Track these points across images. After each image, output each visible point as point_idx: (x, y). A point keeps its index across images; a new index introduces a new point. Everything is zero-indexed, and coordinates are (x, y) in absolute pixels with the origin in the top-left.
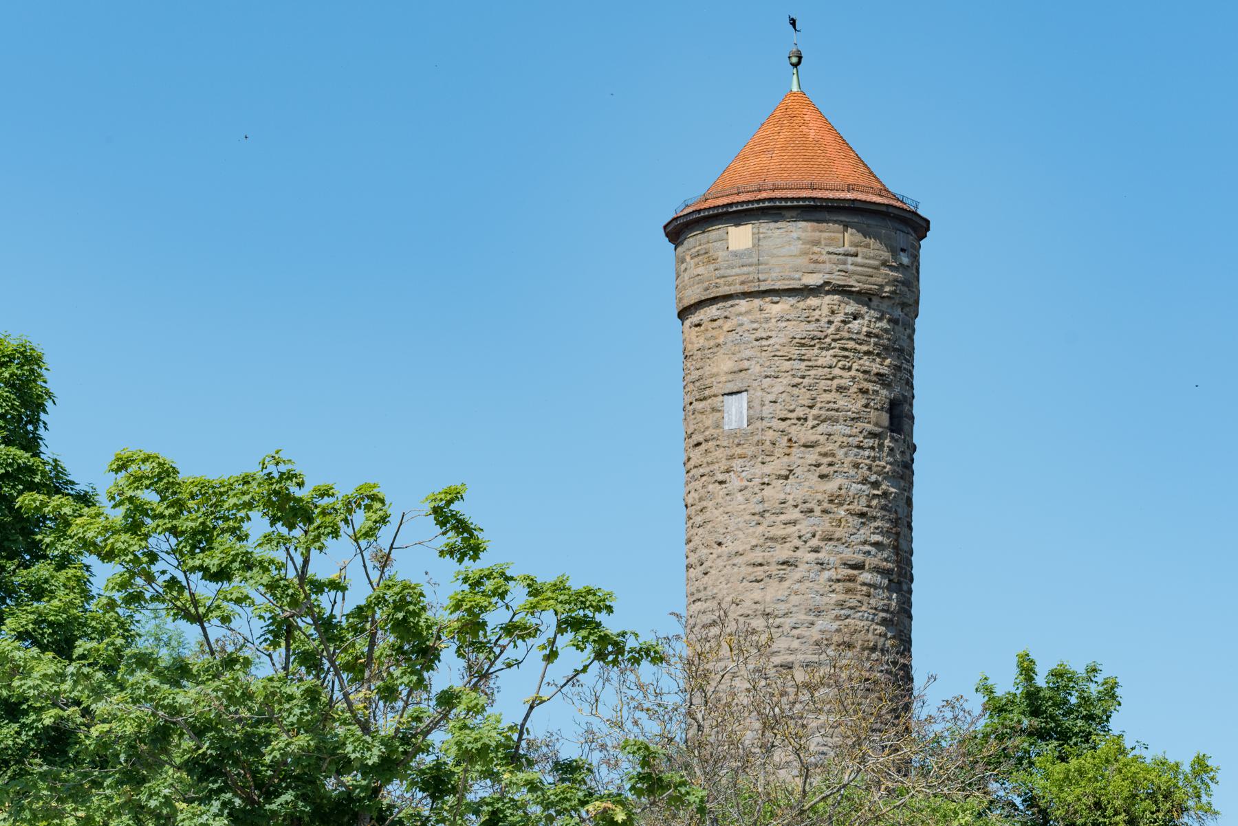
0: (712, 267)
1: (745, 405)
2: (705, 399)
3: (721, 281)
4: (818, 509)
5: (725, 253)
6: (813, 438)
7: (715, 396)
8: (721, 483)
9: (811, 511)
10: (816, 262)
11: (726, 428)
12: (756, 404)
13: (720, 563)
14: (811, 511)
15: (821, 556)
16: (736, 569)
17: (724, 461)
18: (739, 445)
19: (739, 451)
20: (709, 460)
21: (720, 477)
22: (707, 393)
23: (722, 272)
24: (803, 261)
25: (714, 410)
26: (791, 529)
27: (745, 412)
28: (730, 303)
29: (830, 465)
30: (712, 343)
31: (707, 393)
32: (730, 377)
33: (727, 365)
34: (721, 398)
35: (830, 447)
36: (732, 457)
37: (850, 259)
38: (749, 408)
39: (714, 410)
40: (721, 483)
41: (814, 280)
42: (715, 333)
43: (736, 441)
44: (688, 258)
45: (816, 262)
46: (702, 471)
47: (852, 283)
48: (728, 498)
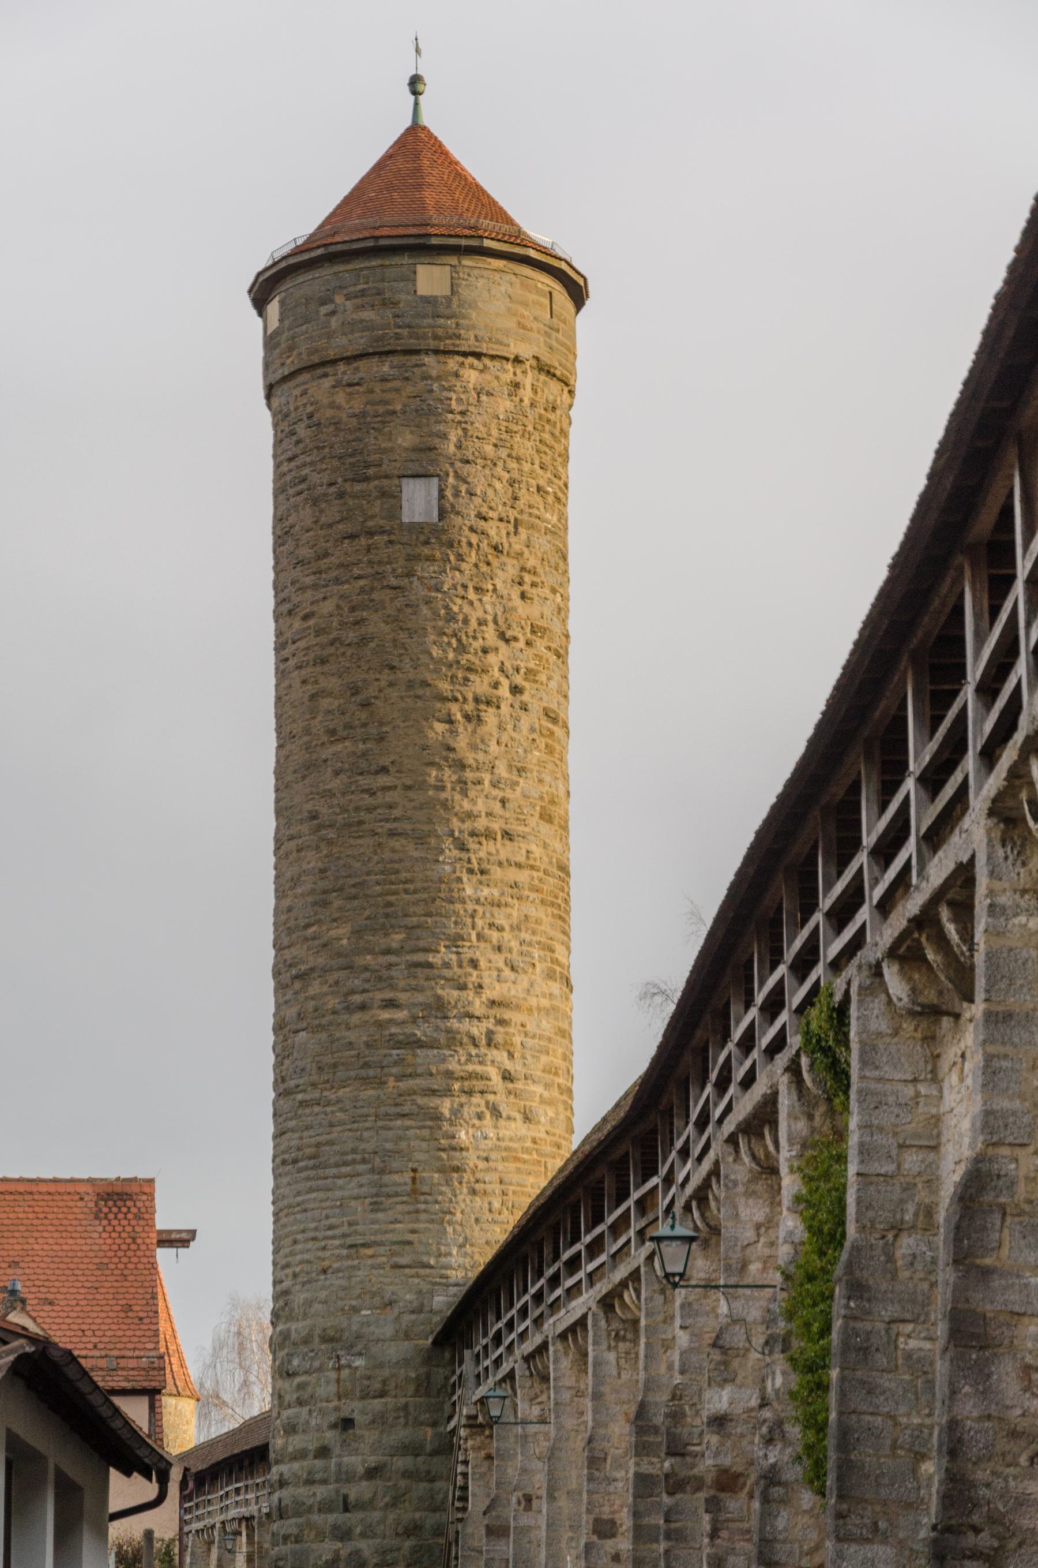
0: (389, 313)
1: (435, 493)
2: (367, 479)
3: (405, 332)
4: (521, 644)
5: (409, 298)
6: (517, 547)
7: (387, 477)
8: (395, 588)
9: (516, 639)
10: (524, 328)
11: (406, 519)
12: (449, 493)
13: (394, 694)
14: (516, 639)
15: (526, 697)
16: (420, 704)
17: (402, 562)
18: (427, 543)
19: (426, 551)
20: (376, 559)
21: (394, 582)
22: (371, 472)
23: (407, 320)
24: (511, 324)
25: (384, 494)
26: (492, 659)
27: (435, 503)
28: (414, 359)
29: (534, 585)
30: (381, 409)
31: (371, 472)
32: (414, 456)
33: (406, 439)
34: (396, 481)
35: (531, 563)
36: (417, 558)
37: (554, 334)
38: (442, 496)
39: (384, 494)
40: (395, 588)
41: (525, 351)
42: (388, 396)
43: (422, 538)
44: (339, 299)
45: (524, 328)
46: (356, 571)
47: (557, 365)
48: (409, 610)
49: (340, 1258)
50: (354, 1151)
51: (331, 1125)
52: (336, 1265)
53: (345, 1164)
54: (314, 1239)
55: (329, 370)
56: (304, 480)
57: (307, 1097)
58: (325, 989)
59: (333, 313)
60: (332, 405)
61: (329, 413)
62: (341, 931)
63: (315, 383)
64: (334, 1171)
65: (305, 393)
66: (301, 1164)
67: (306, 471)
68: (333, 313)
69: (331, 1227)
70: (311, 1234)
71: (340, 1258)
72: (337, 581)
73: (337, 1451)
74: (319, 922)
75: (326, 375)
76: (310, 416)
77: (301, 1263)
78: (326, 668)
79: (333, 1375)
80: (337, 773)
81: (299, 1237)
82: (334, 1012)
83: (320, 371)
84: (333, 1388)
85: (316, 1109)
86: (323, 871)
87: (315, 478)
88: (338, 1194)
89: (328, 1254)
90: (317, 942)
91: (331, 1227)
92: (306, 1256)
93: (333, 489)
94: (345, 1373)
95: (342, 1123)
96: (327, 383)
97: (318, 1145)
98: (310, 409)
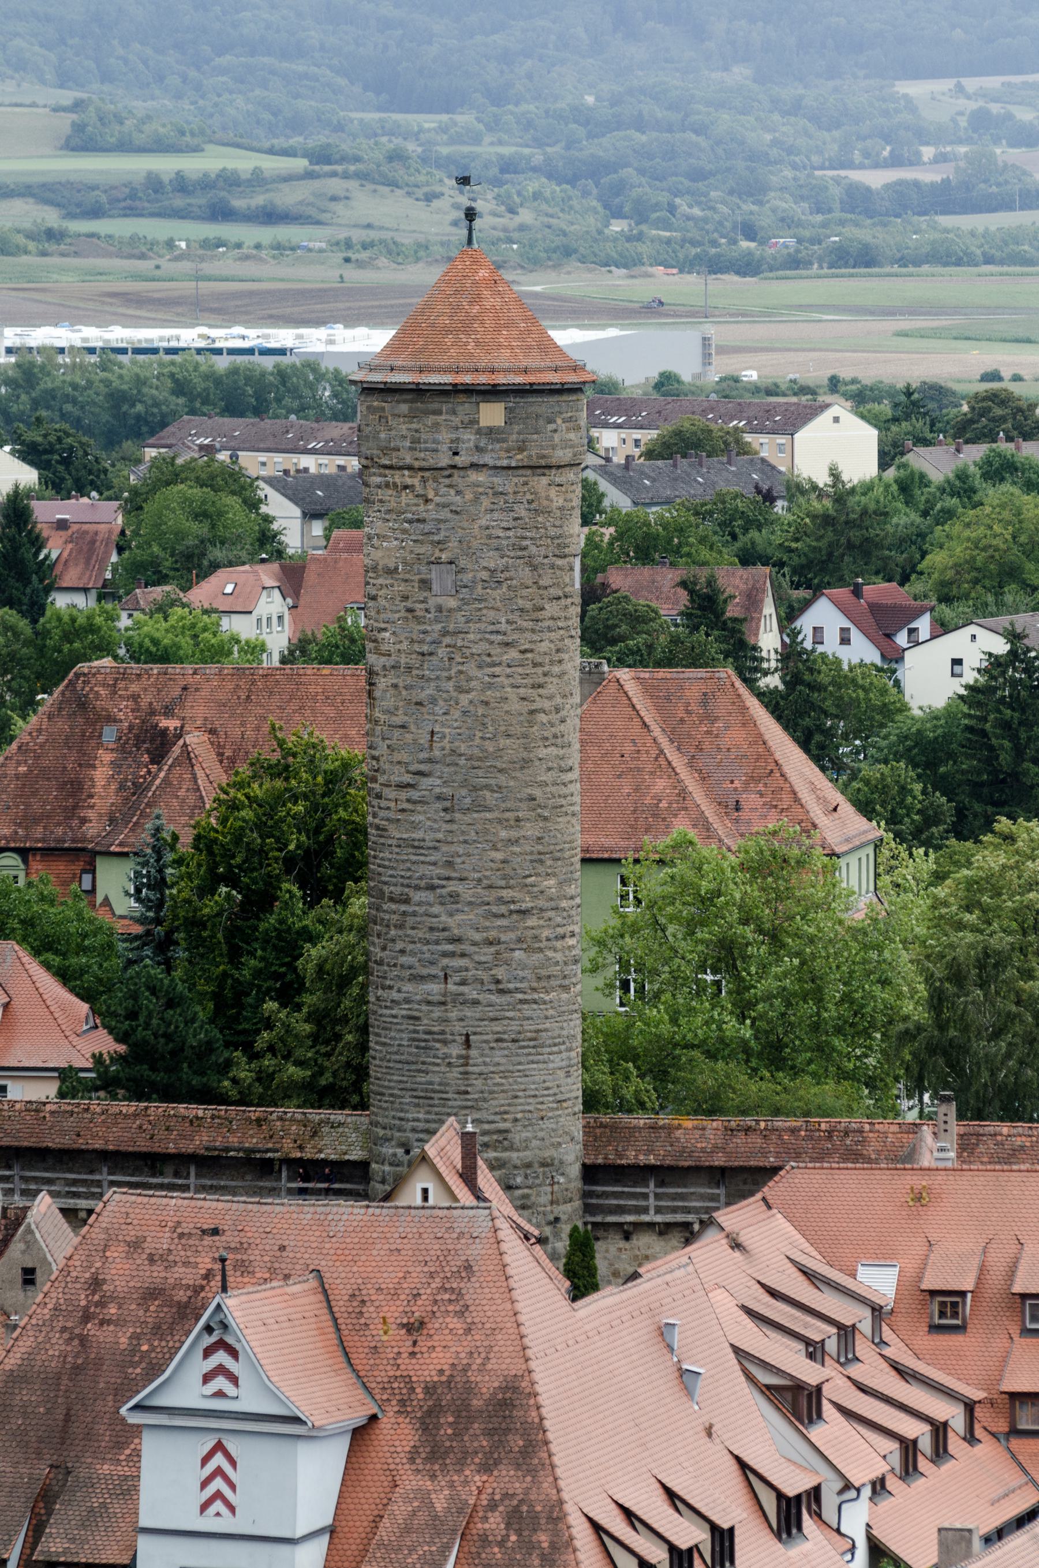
44: (559, 421)
49: (552, 1109)
50: (559, 1036)
51: (547, 1018)
52: (550, 1114)
53: (555, 1045)
54: (535, 1096)
55: (546, 471)
56: (525, 548)
57: (526, 997)
58: (541, 922)
59: (555, 431)
60: (548, 498)
61: (545, 503)
62: (552, 882)
63: (536, 478)
64: (548, 1050)
65: (526, 484)
66: (522, 1043)
67: (528, 542)
68: (555, 431)
69: (547, 1089)
70: (533, 1093)
71: (552, 1109)
72: (550, 629)
73: (551, 1239)
74: (537, 875)
75: (544, 475)
76: (530, 502)
77: (523, 1111)
78: (540, 691)
79: (549, 1189)
80: (549, 769)
81: (520, 1094)
82: (548, 940)
83: (539, 471)
84: (549, 1197)
85: (535, 1006)
86: (539, 838)
87: (533, 549)
88: (551, 1065)
89: (544, 1107)
90: (535, 889)
91: (547, 1089)
92: (527, 1108)
93: (546, 561)
94: (556, 1187)
95: (552, 1017)
96: (544, 480)
97: (538, 1031)
98: (529, 497)
